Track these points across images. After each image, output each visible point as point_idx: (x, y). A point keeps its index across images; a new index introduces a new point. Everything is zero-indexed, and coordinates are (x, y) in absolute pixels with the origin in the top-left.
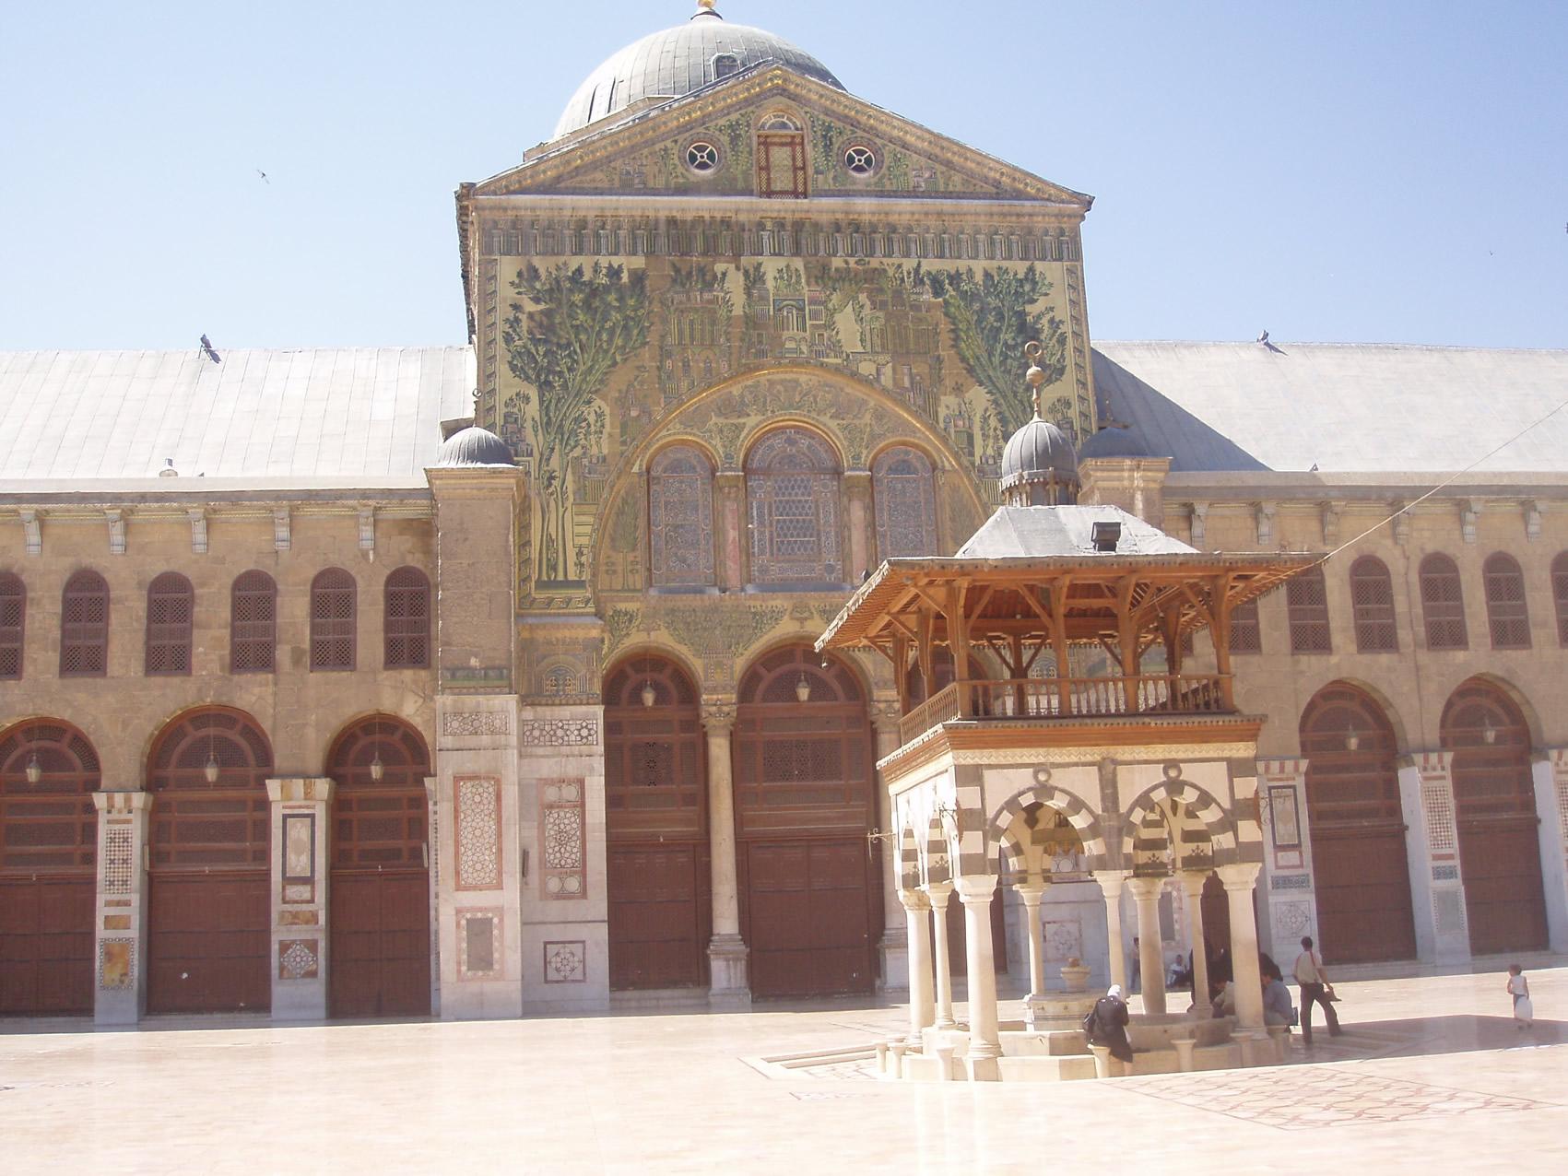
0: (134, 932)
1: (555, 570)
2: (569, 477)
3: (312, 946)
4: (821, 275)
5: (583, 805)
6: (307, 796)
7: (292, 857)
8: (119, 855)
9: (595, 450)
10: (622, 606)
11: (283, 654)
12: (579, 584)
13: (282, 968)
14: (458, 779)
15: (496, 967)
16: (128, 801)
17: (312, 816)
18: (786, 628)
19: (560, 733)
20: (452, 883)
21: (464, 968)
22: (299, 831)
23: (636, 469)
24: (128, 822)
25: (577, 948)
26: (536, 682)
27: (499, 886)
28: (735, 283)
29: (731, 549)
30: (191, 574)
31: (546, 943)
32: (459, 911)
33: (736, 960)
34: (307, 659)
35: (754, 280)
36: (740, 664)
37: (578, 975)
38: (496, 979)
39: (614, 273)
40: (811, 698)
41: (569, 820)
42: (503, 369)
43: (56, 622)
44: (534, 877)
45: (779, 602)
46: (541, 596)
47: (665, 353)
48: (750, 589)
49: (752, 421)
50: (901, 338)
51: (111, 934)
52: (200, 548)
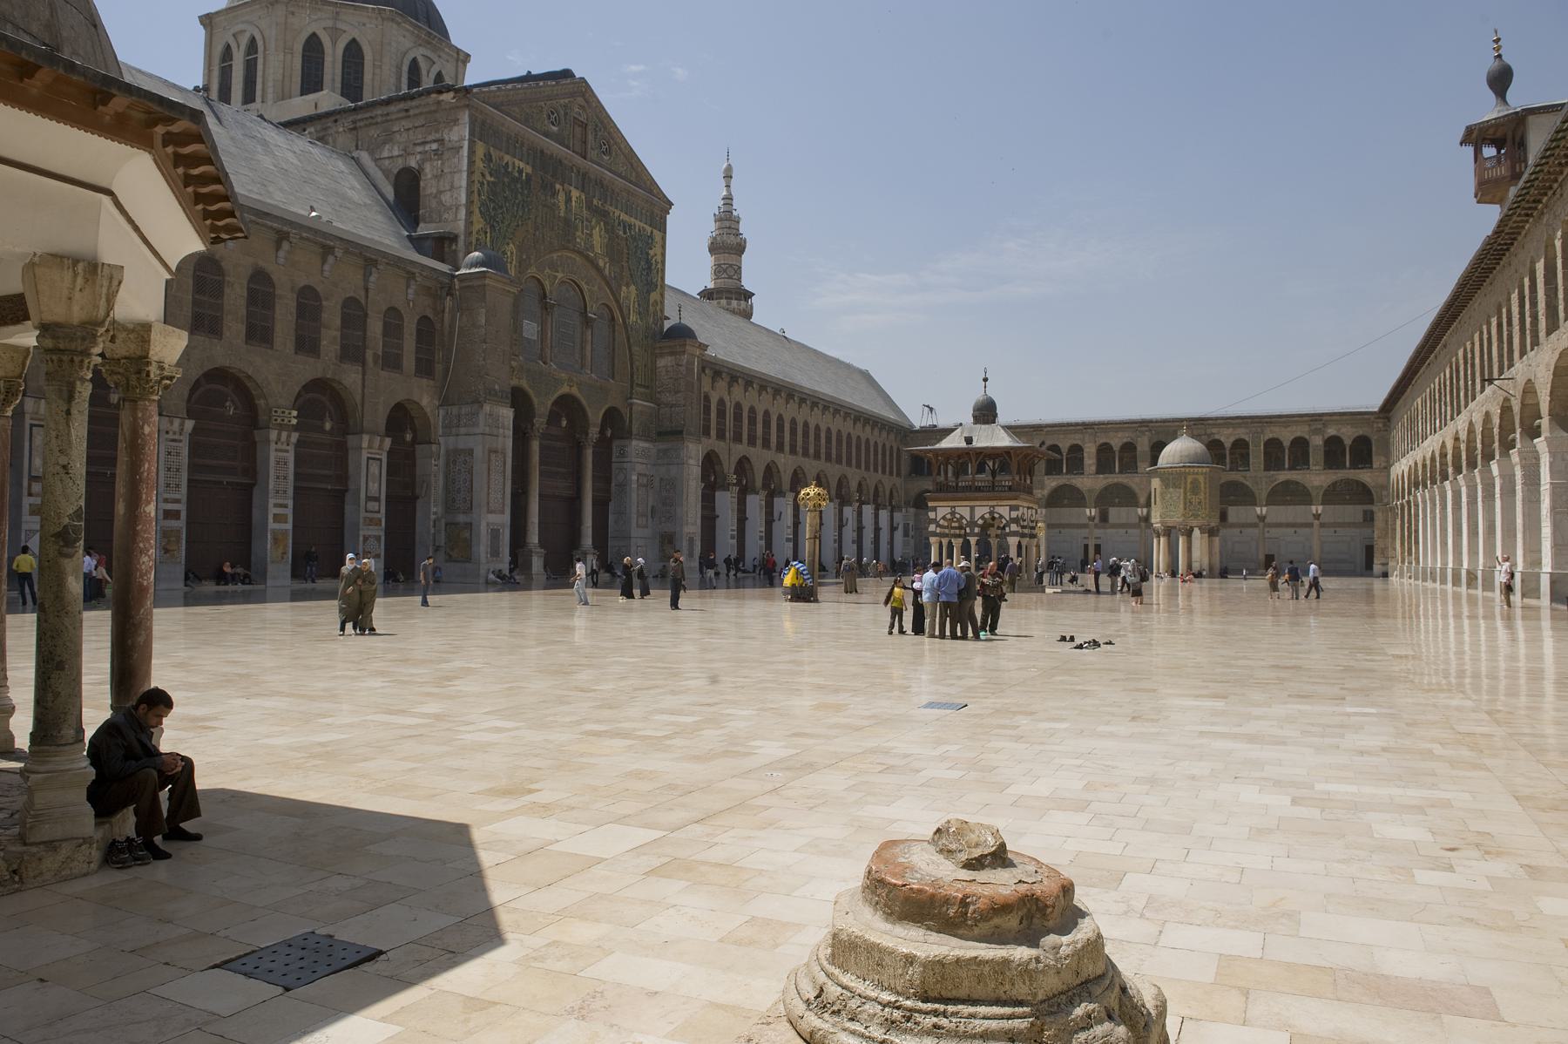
0: (289, 526)
3: (378, 538)
4: (589, 206)
6: (380, 448)
8: (282, 473)
11: (369, 354)
16: (289, 436)
18: (565, 389)
22: (374, 468)
28: (562, 197)
35: (568, 200)
39: (520, 171)
42: (477, 211)
47: (537, 229)
49: (560, 275)
50: (612, 252)
51: (277, 526)
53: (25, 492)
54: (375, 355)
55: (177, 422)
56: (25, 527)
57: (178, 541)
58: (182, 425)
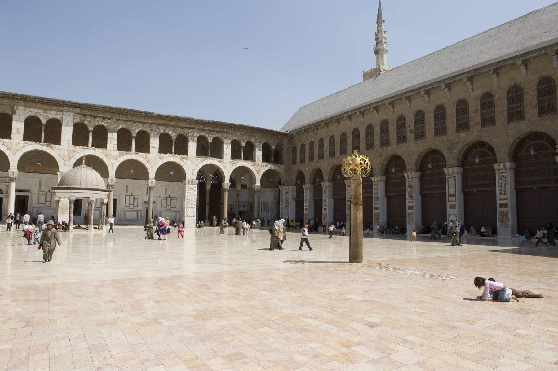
43: (535, 98)
53: (447, 201)
55: (502, 165)
56: (448, 213)
57: (507, 217)
58: (504, 165)
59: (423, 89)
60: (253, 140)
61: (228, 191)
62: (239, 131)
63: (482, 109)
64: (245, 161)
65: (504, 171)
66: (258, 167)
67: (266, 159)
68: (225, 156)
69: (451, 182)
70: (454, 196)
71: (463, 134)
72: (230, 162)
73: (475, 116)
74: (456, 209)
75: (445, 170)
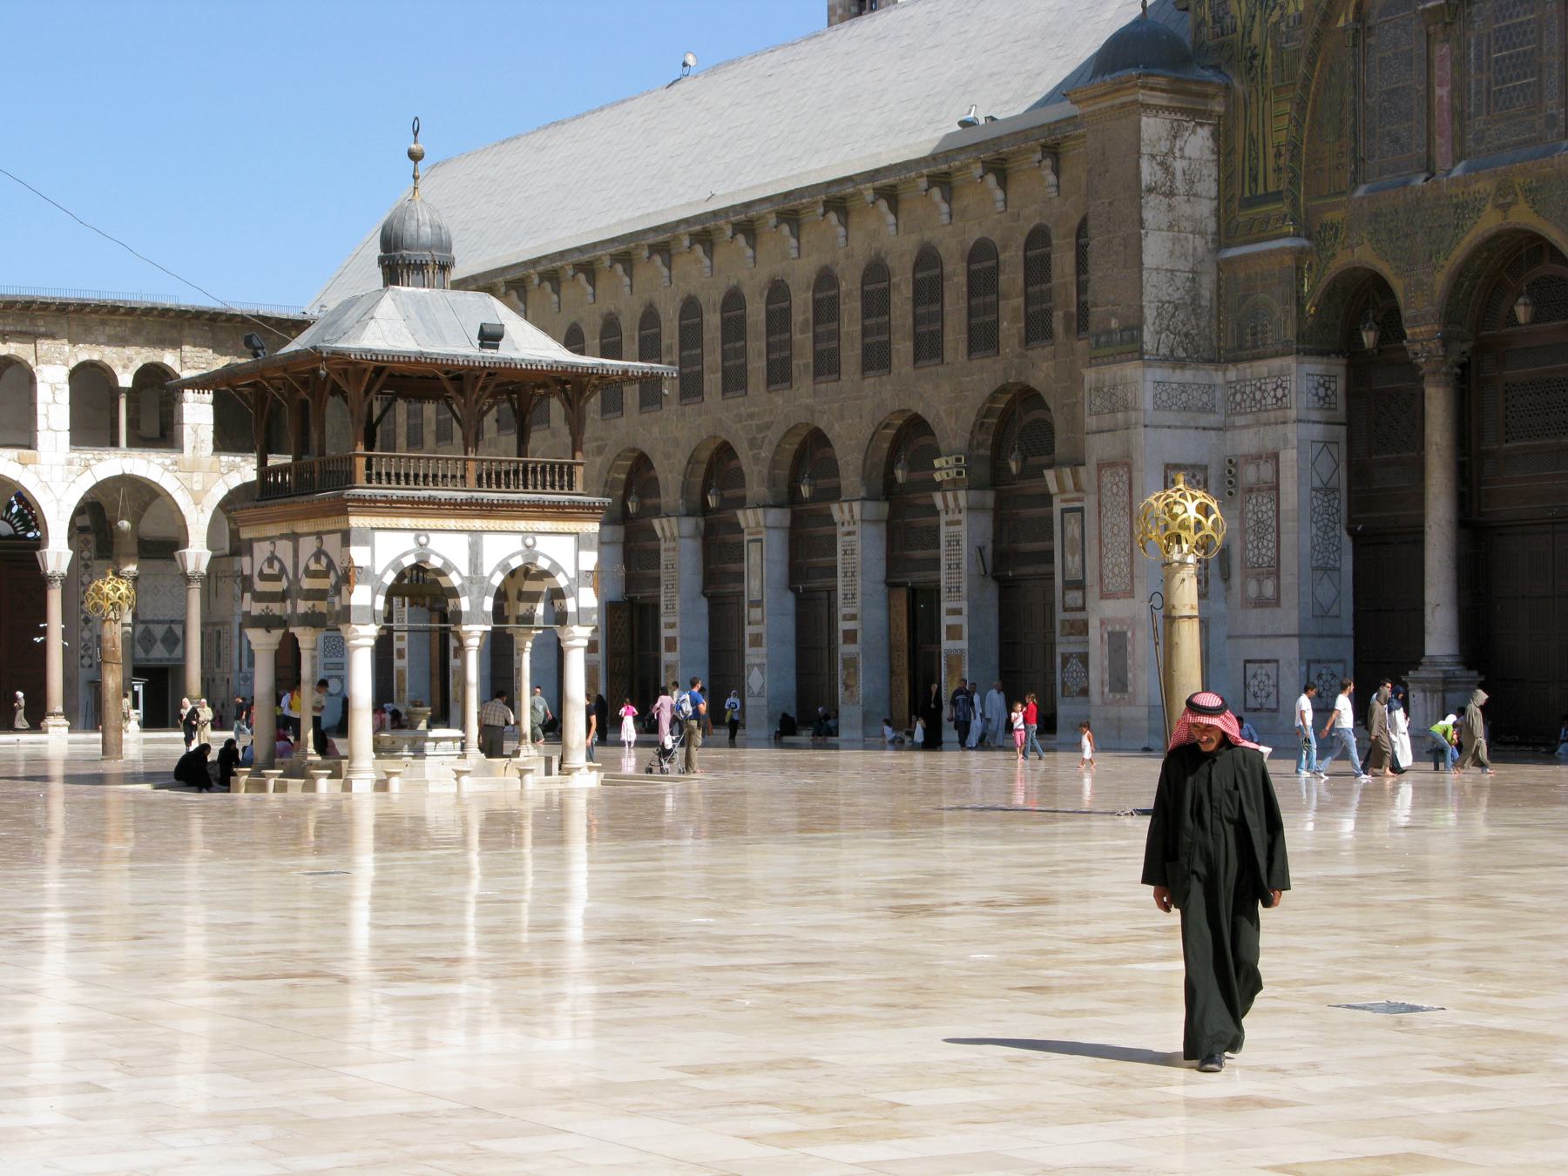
1: (1256, 180)
2: (1270, 52)
5: (1276, 487)
6: (1078, 487)
7: (1069, 558)
9: (1291, 9)
10: (1328, 217)
12: (1277, 196)
13: (1064, 684)
14: (1100, 466)
15: (1130, 689)
16: (956, 499)
17: (1081, 510)
18: (1489, 222)
19: (1258, 395)
20: (1097, 589)
21: (1106, 690)
22: (1073, 530)
23: (1341, 23)
24: (958, 523)
25: (1270, 668)
26: (1225, 334)
27: (1130, 594)
29: (1442, 118)
30: (995, 238)
31: (1247, 661)
32: (1102, 623)
33: (1434, 691)
34: (1074, 325)
36: (1440, 280)
37: (1272, 703)
38: (1130, 704)
40: (1535, 319)
41: (1267, 506)
43: (909, 307)
44: (1236, 580)
45: (1484, 185)
46: (1243, 216)
48: (1458, 171)
52: (1000, 206)
54: (1066, 315)
56: (747, 661)
59: (682, 230)
60: (169, 358)
61: (67, 582)
62: (103, 323)
63: (816, 322)
64: (136, 452)
65: (850, 528)
66: (197, 477)
67: (227, 438)
68: (43, 437)
69: (753, 556)
70: (758, 604)
71: (778, 399)
72: (70, 463)
73: (803, 341)
74: (763, 650)
75: (740, 513)
